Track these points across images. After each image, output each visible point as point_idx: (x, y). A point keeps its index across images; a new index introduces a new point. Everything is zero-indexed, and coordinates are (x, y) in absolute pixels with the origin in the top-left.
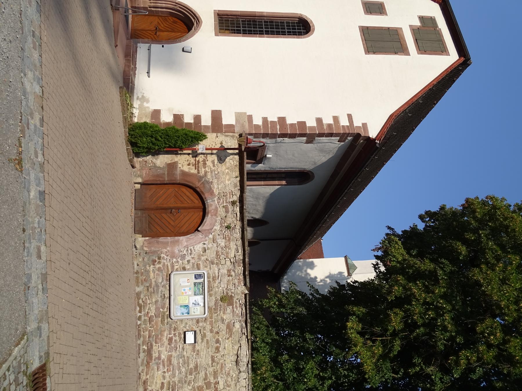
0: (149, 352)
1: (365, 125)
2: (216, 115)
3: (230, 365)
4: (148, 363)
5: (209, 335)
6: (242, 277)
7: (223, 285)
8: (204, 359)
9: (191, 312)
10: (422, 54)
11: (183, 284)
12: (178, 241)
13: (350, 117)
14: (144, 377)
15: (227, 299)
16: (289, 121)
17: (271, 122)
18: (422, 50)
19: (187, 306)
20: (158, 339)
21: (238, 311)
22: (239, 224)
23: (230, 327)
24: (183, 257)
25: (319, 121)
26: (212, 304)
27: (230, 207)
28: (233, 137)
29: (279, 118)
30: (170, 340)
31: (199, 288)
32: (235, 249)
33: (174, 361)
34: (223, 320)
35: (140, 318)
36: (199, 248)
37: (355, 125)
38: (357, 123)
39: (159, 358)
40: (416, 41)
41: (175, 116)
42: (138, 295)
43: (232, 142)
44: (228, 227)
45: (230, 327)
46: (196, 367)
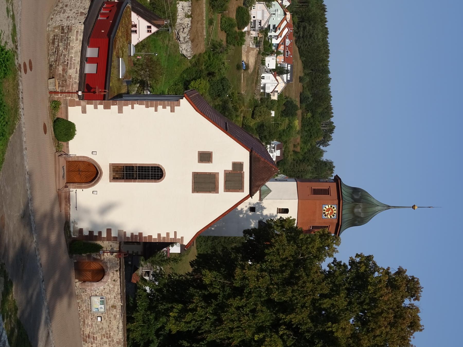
0: (84, 322)
2: (109, 231)
3: (115, 328)
4: (84, 326)
5: (107, 318)
6: (120, 299)
7: (112, 302)
8: (105, 325)
9: (100, 311)
10: (227, 191)
11: (96, 301)
12: (93, 285)
13: (175, 233)
14: (83, 329)
15: (114, 307)
16: (144, 235)
17: (135, 235)
18: (228, 188)
19: (97, 309)
20: (87, 318)
21: (119, 311)
22: (119, 279)
23: (115, 316)
24: (96, 291)
25: (159, 235)
26: (108, 308)
28: (116, 243)
29: (139, 233)
30: (92, 319)
31: (102, 303)
32: (117, 288)
33: (94, 325)
34: (112, 314)
35: (80, 311)
36: (102, 288)
37: (177, 238)
38: (179, 237)
39: (88, 324)
40: (226, 181)
42: (78, 303)
44: (114, 280)
45: (115, 316)
46: (102, 328)
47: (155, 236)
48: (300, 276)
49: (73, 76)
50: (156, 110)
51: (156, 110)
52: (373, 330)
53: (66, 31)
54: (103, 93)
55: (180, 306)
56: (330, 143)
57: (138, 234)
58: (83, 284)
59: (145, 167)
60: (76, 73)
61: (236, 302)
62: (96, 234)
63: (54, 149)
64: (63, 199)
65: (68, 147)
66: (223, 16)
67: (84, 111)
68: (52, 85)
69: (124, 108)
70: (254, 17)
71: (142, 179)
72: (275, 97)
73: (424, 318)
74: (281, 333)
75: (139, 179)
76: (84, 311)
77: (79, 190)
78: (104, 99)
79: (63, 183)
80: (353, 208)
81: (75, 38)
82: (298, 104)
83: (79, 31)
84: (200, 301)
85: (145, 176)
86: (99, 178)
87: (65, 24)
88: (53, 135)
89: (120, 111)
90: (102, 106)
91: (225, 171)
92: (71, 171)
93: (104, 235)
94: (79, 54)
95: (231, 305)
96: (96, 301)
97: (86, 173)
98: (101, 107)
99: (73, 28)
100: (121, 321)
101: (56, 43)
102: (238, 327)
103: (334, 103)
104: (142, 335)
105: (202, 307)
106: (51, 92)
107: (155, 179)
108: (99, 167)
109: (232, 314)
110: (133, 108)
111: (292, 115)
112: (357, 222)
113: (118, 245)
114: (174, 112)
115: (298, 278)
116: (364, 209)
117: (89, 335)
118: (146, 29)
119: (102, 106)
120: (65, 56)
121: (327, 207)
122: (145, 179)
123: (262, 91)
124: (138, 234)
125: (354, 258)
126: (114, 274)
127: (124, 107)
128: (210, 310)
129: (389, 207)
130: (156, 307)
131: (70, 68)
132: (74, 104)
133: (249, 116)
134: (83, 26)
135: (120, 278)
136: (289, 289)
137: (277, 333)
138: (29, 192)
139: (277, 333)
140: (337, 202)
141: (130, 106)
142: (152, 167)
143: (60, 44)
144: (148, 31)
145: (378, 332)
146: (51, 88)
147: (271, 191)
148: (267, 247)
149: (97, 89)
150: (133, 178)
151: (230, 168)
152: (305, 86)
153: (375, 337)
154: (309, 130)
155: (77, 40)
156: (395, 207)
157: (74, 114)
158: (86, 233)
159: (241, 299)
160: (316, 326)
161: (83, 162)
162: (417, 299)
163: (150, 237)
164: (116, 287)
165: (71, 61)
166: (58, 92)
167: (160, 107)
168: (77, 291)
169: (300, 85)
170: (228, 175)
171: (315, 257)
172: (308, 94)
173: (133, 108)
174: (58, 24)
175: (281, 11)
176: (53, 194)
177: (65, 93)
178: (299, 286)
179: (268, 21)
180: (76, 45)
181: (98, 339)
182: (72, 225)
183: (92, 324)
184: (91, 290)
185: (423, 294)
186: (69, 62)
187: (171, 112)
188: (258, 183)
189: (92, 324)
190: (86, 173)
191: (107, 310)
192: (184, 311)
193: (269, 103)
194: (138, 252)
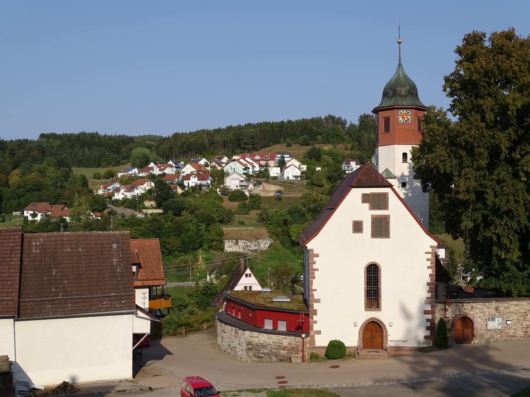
0: (512, 336)
1: (431, 247)
2: (426, 312)
3: (517, 308)
7: (492, 310)
8: (515, 317)
11: (492, 325)
12: (477, 328)
13: (426, 253)
14: (519, 338)
15: (497, 309)
16: (429, 281)
18: (385, 207)
20: (508, 333)
21: (501, 305)
24: (482, 325)
25: (429, 267)
26: (498, 314)
27: (464, 307)
29: (427, 285)
31: (493, 319)
33: (515, 327)
36: (479, 319)
38: (430, 250)
40: (379, 208)
41: (427, 329)
42: (494, 341)
43: (440, 306)
44: (472, 308)
45: (506, 308)
47: (430, 271)
48: (464, 141)
49: (289, 341)
50: (317, 270)
51: (317, 270)
52: (514, 73)
53: (251, 347)
54: (303, 316)
55: (495, 248)
56: (343, 119)
57: (428, 287)
58: (476, 336)
59: (367, 279)
60: (286, 338)
61: (490, 198)
62: (429, 324)
63: (353, 359)
64: (397, 352)
65: (351, 347)
66: (237, 213)
67: (319, 332)
68: (297, 359)
69: (316, 297)
70: (237, 186)
71: (378, 282)
72: (304, 168)
73: (502, 28)
74: (519, 156)
75: (378, 285)
76: (502, 336)
77: (389, 338)
78: (308, 315)
79: (382, 353)
80: (401, 96)
81: (256, 339)
82: (310, 147)
83: (250, 335)
84: (490, 230)
85: (376, 279)
86: (378, 320)
87: (244, 347)
88: (340, 360)
89: (318, 301)
90: (314, 316)
91: (369, 209)
92: (372, 345)
93: (430, 317)
94: (270, 335)
95: (493, 202)
96: (492, 325)
97: (374, 331)
98: (315, 318)
99: (248, 340)
100: (511, 303)
101: (261, 355)
102: (514, 196)
103: (308, 117)
104: (523, 284)
105: (495, 229)
106: (303, 361)
107: (378, 271)
108: (368, 320)
109: (502, 201)
110: (315, 290)
111: (320, 152)
112: (414, 92)
113: (439, 304)
114: (318, 254)
115: (467, 142)
116: (402, 86)
117: (525, 332)
118: (248, 278)
119: (314, 316)
120: (271, 348)
121: (401, 119)
122: (378, 280)
123: (299, 179)
124: (428, 287)
125: (447, 93)
126: (466, 309)
127: (315, 298)
128: (498, 221)
129: (400, 65)
130: (496, 270)
131: (282, 344)
132: (313, 341)
133: (321, 189)
134: (246, 332)
135: (469, 303)
136: (477, 150)
137: (518, 160)
138: (392, 383)
139: (518, 160)
140: (396, 111)
141: (314, 292)
142: (367, 274)
143: (262, 352)
144: (250, 276)
145: (517, 68)
146: (299, 360)
147: (387, 169)
148: (438, 171)
149: (300, 321)
150: (378, 291)
151: (367, 205)
152: (294, 141)
153: (521, 71)
154: (332, 137)
155: (258, 337)
156: (400, 59)
157: (322, 341)
158: (428, 333)
159: (487, 193)
160: (512, 125)
161: (363, 334)
162: (484, 35)
163: (430, 275)
164: (478, 306)
165: (276, 343)
166: (303, 355)
167: (315, 266)
168: (483, 342)
169: (293, 146)
170: (373, 207)
171: (447, 127)
172: (301, 139)
173: (315, 290)
174: (245, 353)
175: (232, 164)
176: (393, 361)
177: (303, 349)
178: (475, 142)
179: (240, 175)
180: (262, 338)
181: (528, 324)
182: (421, 346)
183: (514, 329)
184: (482, 329)
185: (480, 29)
186: (277, 344)
187: (318, 257)
188: (380, 180)
189: (514, 329)
190: (374, 331)
191: (500, 315)
192: (500, 245)
193: (309, 172)
194: (445, 287)
